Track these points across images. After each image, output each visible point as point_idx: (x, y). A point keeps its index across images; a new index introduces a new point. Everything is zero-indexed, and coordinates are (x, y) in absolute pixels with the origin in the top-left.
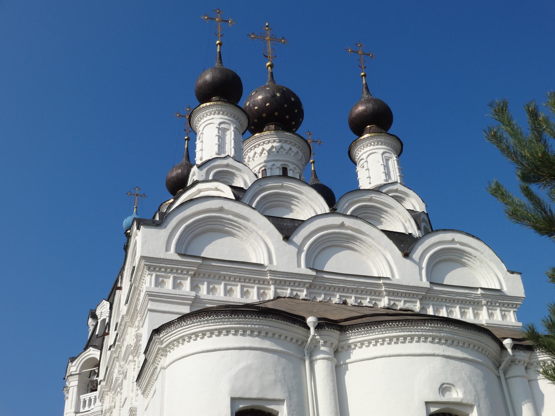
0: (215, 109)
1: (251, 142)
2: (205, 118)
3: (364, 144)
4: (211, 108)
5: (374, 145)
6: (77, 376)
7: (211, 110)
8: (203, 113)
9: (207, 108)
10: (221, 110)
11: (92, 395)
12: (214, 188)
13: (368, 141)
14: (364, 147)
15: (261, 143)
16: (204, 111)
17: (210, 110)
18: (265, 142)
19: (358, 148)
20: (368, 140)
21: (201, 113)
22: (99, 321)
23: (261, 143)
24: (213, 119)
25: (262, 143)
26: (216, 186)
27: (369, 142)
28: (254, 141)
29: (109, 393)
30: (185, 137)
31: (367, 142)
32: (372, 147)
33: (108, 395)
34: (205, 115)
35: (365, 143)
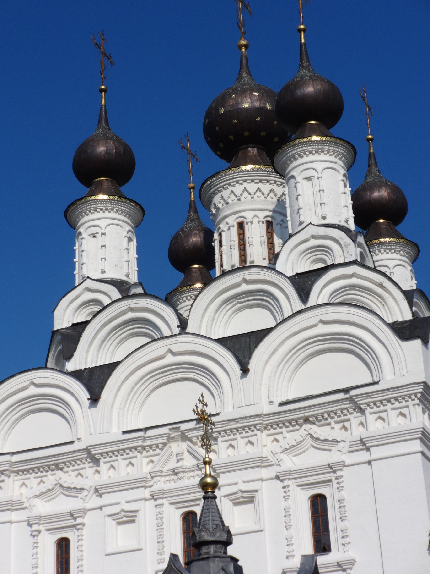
0: (341, 151)
1: (259, 172)
2: (322, 154)
3: (393, 247)
4: (338, 148)
5: (401, 255)
7: (337, 149)
8: (325, 147)
9: (333, 145)
10: (342, 154)
12: (379, 282)
13: (399, 248)
14: (390, 251)
15: (271, 180)
16: (326, 146)
17: (335, 149)
18: (277, 183)
19: (382, 249)
20: (400, 246)
21: (322, 147)
23: (271, 180)
24: (335, 163)
25: (273, 182)
26: (382, 282)
27: (400, 249)
28: (264, 172)
29: (12, 475)
30: (102, 85)
31: (397, 248)
32: (398, 257)
33: (9, 477)
34: (326, 152)
35: (394, 247)
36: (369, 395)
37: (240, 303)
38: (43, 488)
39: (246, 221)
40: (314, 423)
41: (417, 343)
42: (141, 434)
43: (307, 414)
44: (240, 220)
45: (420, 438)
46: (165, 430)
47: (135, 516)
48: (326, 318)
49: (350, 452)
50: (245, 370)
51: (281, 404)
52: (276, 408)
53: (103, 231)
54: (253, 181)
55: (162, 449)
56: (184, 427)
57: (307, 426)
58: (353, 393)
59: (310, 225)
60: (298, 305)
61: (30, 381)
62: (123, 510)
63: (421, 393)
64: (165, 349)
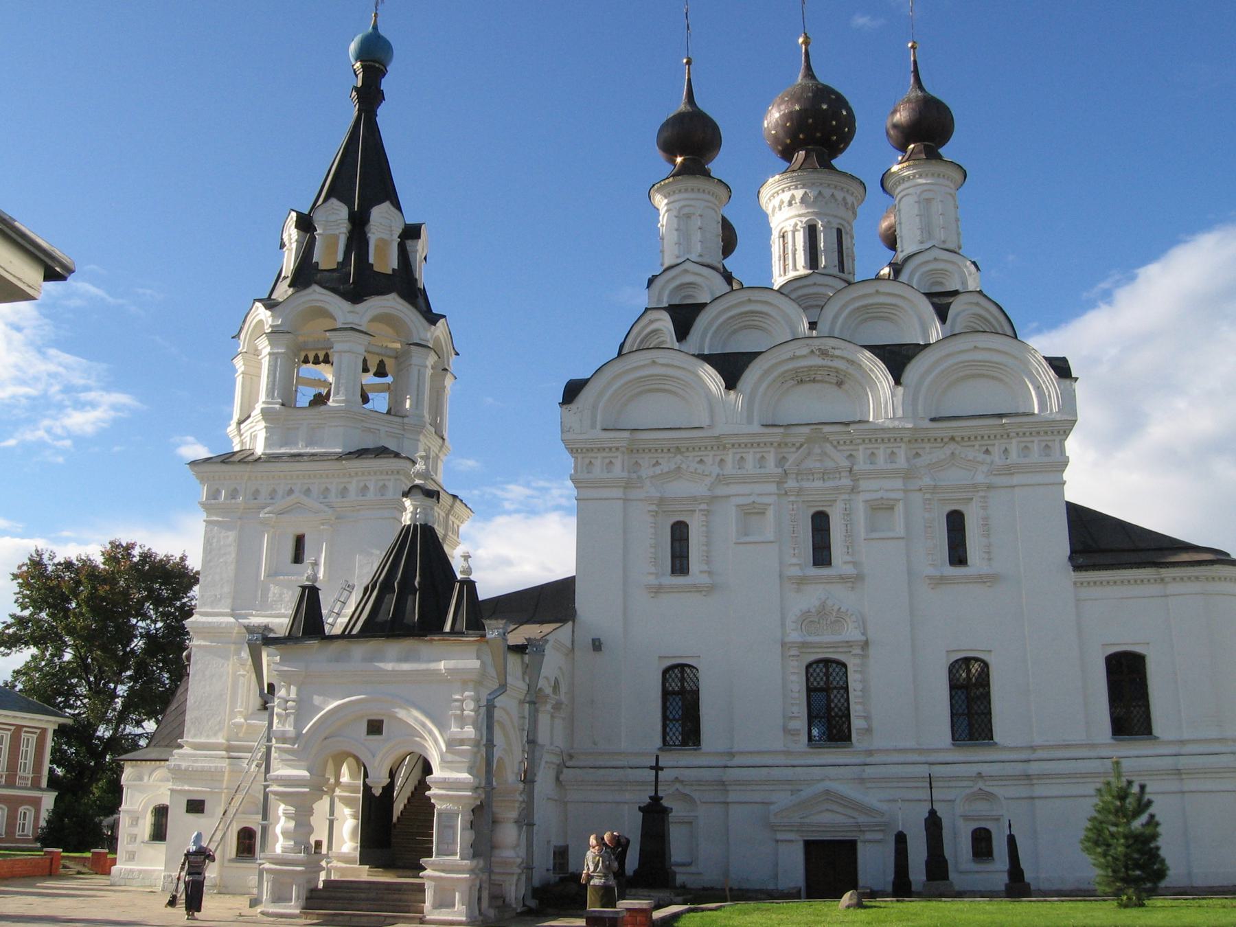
37: (868, 313)
38: (658, 470)
40: (958, 443)
42: (781, 430)
43: (955, 434)
46: (806, 430)
47: (766, 509)
48: (980, 345)
54: (829, 185)
55: (798, 449)
56: (827, 429)
57: (952, 446)
59: (934, 248)
61: (651, 361)
62: (754, 502)
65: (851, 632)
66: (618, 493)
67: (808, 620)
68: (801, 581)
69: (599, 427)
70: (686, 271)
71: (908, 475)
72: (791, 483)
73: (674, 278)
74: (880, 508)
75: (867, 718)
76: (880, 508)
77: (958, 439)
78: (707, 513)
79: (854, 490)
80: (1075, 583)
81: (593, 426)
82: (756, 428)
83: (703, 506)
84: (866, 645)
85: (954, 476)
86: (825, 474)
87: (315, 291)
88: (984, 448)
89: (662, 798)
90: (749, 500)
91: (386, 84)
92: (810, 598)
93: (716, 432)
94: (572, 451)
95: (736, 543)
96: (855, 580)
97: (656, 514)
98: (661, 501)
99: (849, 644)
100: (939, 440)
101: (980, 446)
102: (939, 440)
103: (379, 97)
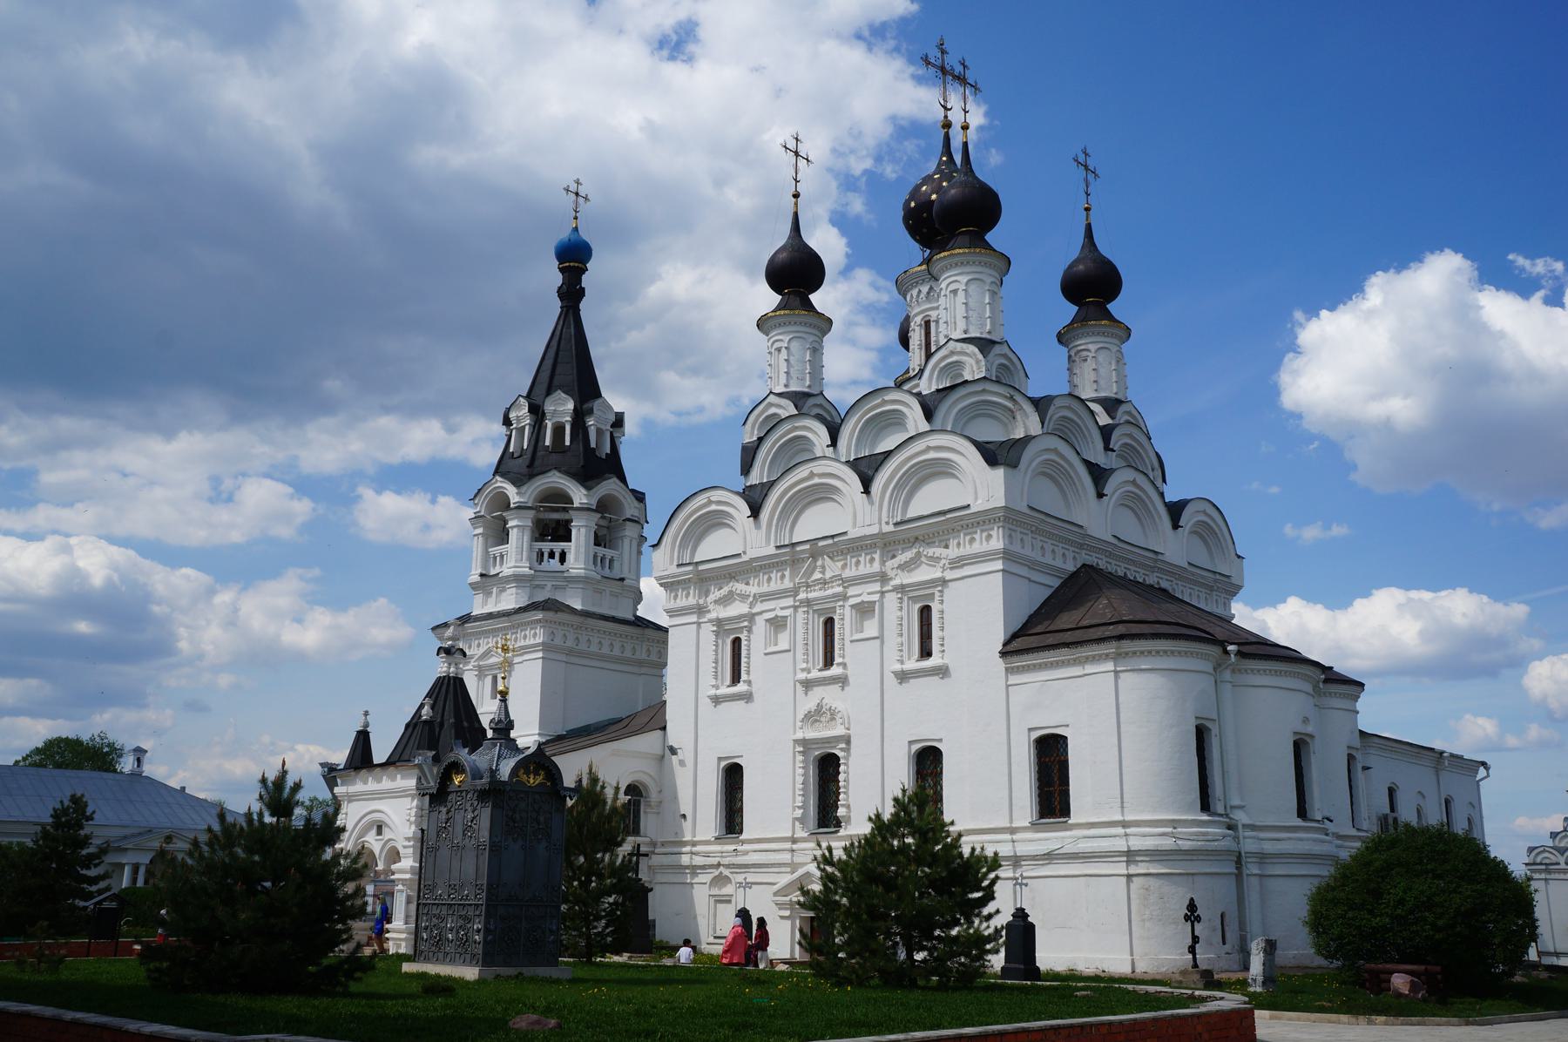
6: (531, 513)
11: (558, 546)
22: (549, 424)
36: (961, 518)
39: (932, 319)
41: (1000, 472)
44: (927, 319)
45: (1003, 558)
46: (807, 547)
48: (932, 444)
49: (951, 569)
50: (867, 491)
51: (896, 524)
52: (891, 528)
53: (786, 345)
56: (821, 543)
58: (949, 516)
60: (924, 426)
63: (1004, 516)
64: (809, 471)
65: (839, 731)
66: (694, 618)
67: (813, 717)
68: (808, 685)
69: (675, 563)
70: (771, 405)
71: (883, 578)
72: (802, 596)
73: (759, 415)
74: (864, 610)
75: (848, 807)
76: (864, 610)
77: (921, 538)
78: (750, 631)
79: (845, 597)
80: (1007, 669)
81: (671, 563)
82: (771, 550)
83: (746, 624)
84: (847, 740)
85: (924, 574)
86: (824, 583)
87: (497, 481)
88: (944, 544)
89: (641, 880)
90: (770, 615)
91: (586, 280)
92: (809, 703)
93: (745, 558)
94: (661, 585)
95: (766, 654)
96: (842, 681)
97: (717, 634)
98: (719, 622)
99: (837, 739)
100: (906, 541)
101: (940, 541)
102: (906, 541)
103: (581, 293)
